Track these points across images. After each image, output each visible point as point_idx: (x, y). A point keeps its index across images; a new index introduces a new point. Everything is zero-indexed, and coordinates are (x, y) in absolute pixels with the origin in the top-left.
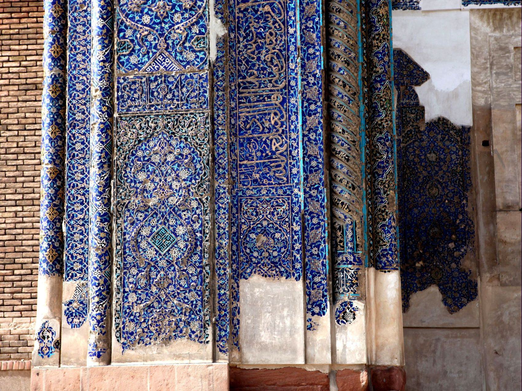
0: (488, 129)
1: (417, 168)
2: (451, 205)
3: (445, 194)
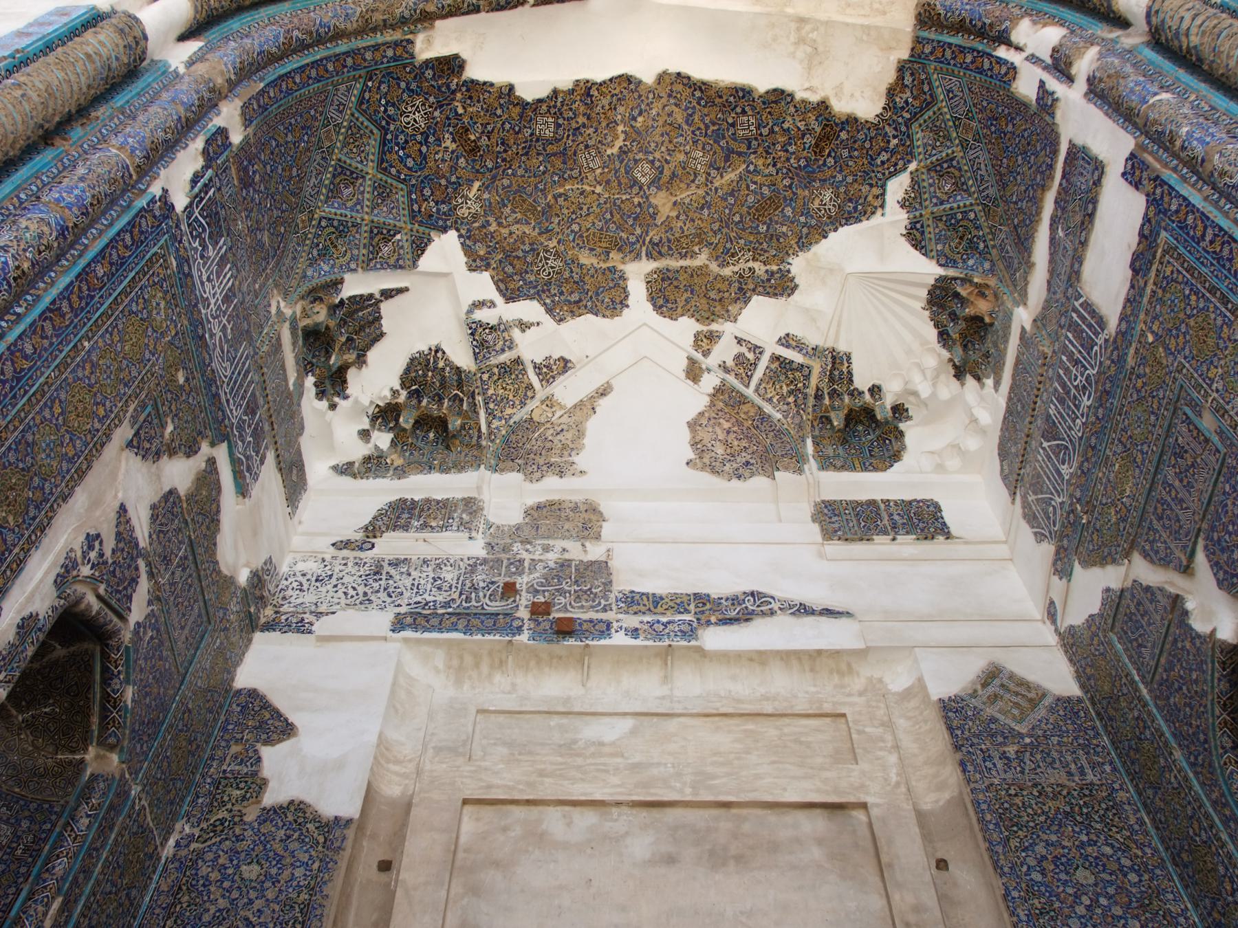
0: (399, 836)
1: (209, 892)
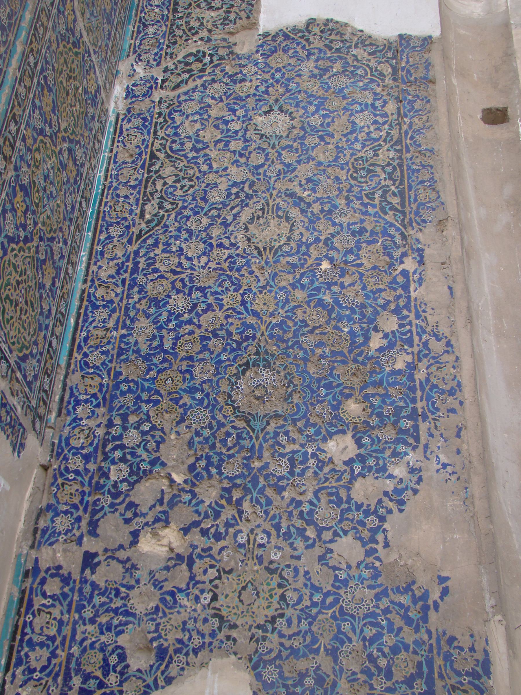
2: (347, 281)
3: (317, 240)
